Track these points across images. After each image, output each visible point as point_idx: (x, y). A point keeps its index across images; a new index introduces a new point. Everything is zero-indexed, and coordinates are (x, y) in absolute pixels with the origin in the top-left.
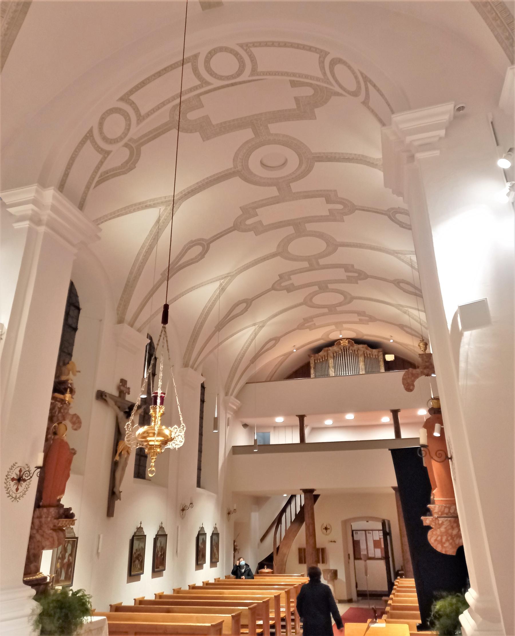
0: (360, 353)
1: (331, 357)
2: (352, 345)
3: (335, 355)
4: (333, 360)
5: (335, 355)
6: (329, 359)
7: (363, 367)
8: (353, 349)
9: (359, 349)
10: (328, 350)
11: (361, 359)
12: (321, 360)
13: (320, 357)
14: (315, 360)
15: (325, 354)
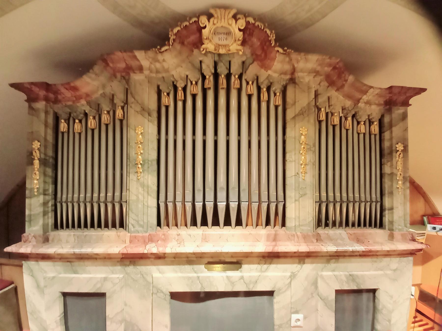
0: (300, 99)
1: (144, 110)
2: (262, 56)
3: (167, 100)
4: (152, 129)
5: (167, 100)
6: (134, 118)
7: (310, 178)
8: (264, 75)
9: (292, 81)
10: (129, 69)
11: (301, 134)
12: (92, 123)
13: (83, 106)
14: (57, 119)
15: (116, 88)
